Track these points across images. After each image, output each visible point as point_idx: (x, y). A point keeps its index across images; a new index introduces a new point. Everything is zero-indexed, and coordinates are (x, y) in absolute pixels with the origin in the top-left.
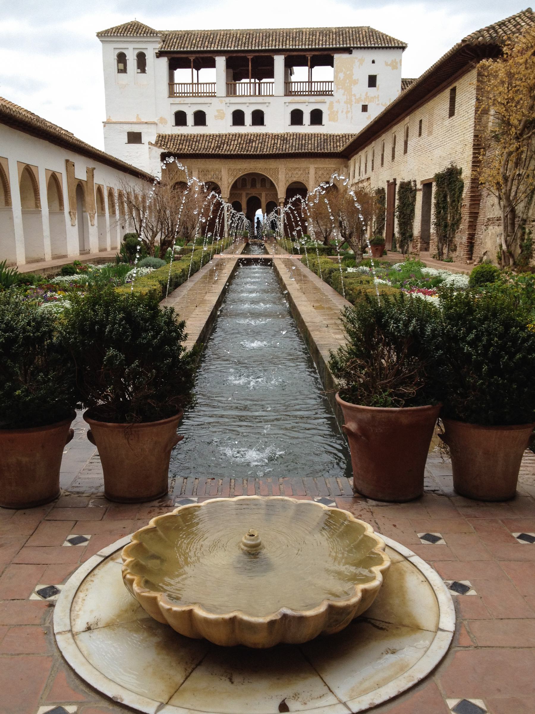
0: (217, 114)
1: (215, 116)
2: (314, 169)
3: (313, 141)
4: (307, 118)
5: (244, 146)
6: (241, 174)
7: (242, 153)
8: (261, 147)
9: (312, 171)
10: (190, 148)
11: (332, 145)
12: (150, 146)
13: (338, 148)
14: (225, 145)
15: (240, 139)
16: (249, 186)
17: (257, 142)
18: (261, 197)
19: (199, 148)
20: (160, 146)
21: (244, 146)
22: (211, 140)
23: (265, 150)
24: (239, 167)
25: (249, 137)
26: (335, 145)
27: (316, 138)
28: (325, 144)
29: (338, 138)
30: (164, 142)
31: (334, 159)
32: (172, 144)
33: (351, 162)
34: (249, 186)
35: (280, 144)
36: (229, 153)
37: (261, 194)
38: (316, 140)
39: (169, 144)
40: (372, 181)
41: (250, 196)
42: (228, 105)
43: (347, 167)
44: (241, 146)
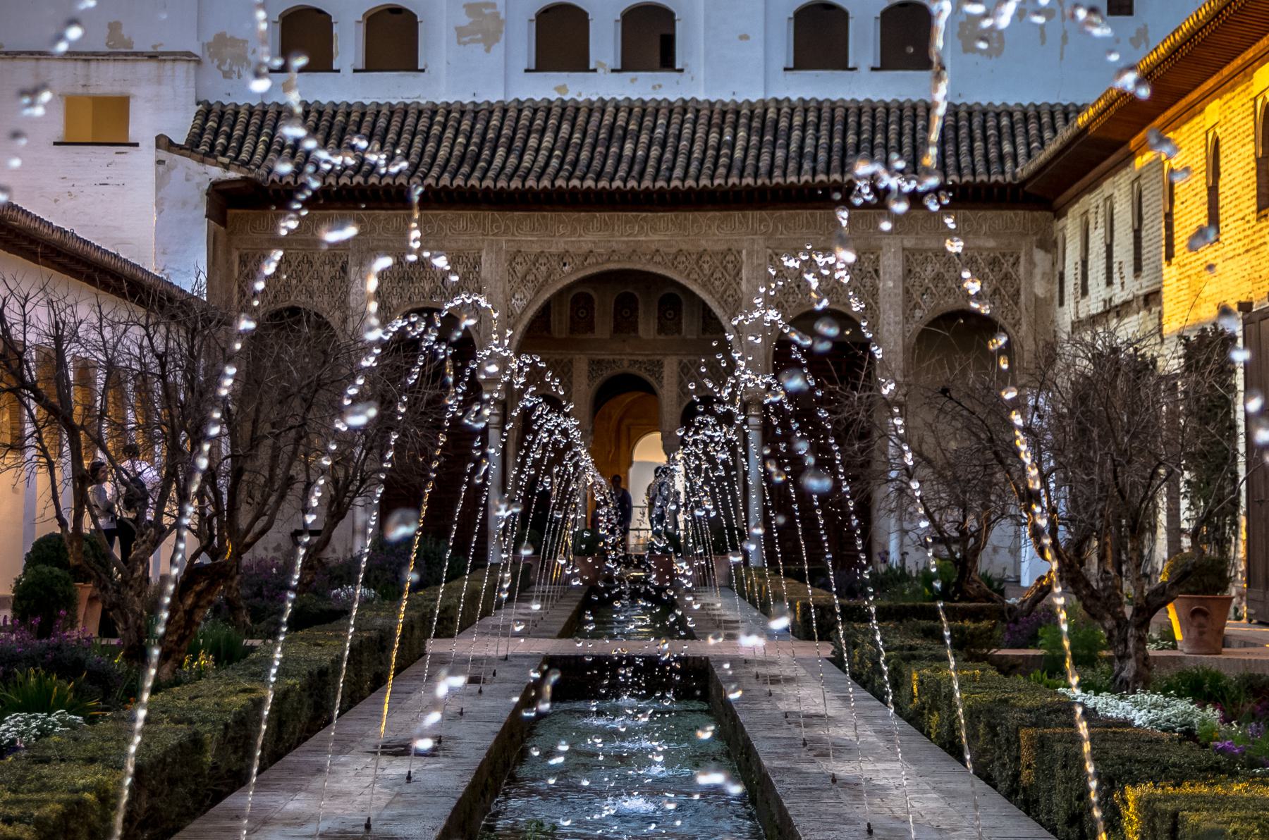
0: (464, 20)
1: (460, 32)
3: (893, 136)
5: (584, 155)
6: (568, 275)
7: (575, 182)
8: (660, 160)
11: (978, 153)
12: (164, 155)
13: (1009, 165)
14: (501, 151)
15: (565, 127)
17: (644, 138)
18: (660, 379)
20: (210, 155)
21: (584, 155)
22: (436, 129)
23: (678, 172)
24: (558, 245)
25: (608, 119)
26: (993, 154)
27: (907, 124)
29: (1005, 121)
30: (229, 137)
32: (261, 147)
33: (1070, 226)
34: (603, 329)
35: (746, 149)
36: (516, 183)
37: (660, 364)
38: (907, 130)
39: (247, 146)
41: (607, 374)
43: (1051, 245)
44: (570, 157)
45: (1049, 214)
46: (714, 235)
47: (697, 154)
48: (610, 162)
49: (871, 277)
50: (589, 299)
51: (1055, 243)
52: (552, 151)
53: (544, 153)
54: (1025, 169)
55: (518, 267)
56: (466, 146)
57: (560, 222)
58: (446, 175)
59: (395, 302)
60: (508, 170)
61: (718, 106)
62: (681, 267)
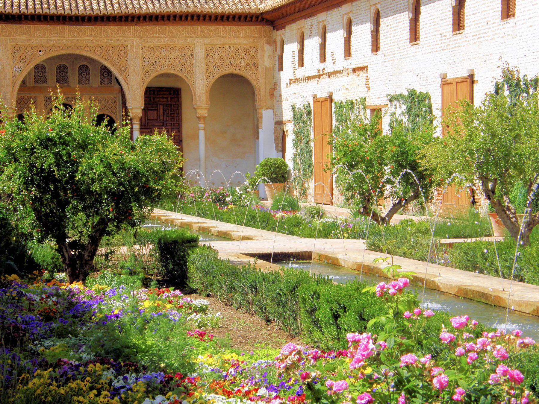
2: (204, 49)
9: (200, 52)
31: (244, 28)
40: (371, 73)
45: (271, 28)
46: (114, 37)
49: (190, 58)
50: (43, 67)
51: (275, 42)
54: (263, 7)
57: (37, 30)
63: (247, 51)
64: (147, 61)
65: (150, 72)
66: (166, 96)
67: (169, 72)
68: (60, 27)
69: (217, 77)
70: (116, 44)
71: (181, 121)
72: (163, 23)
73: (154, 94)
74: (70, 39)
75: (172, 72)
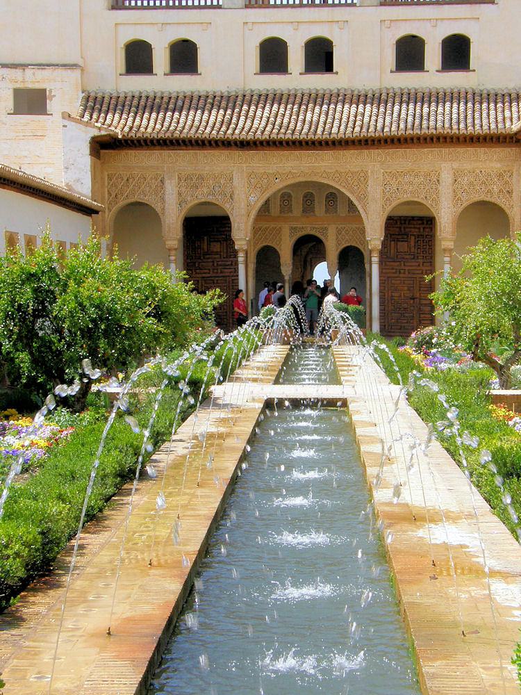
2: (452, 172)
4: (433, 55)
5: (286, 120)
6: (279, 185)
8: (325, 123)
9: (447, 178)
10: (158, 126)
14: (242, 118)
16: (297, 209)
18: (326, 237)
19: (181, 125)
21: (286, 120)
23: (335, 130)
26: (500, 118)
28: (477, 115)
31: (498, 150)
35: (371, 116)
37: (326, 229)
42: (250, 26)
47: (344, 119)
48: (299, 124)
50: (290, 196)
52: (269, 118)
53: (264, 119)
55: (252, 180)
56: (224, 116)
58: (214, 132)
59: (189, 199)
60: (246, 129)
61: (356, 93)
62: (337, 179)
63: (500, 175)
64: (388, 188)
65: (391, 199)
66: (418, 226)
67: (412, 199)
68: (297, 153)
69: (465, 205)
70: (355, 170)
71: (434, 254)
72: (407, 146)
73: (405, 223)
74: (307, 165)
75: (416, 200)
